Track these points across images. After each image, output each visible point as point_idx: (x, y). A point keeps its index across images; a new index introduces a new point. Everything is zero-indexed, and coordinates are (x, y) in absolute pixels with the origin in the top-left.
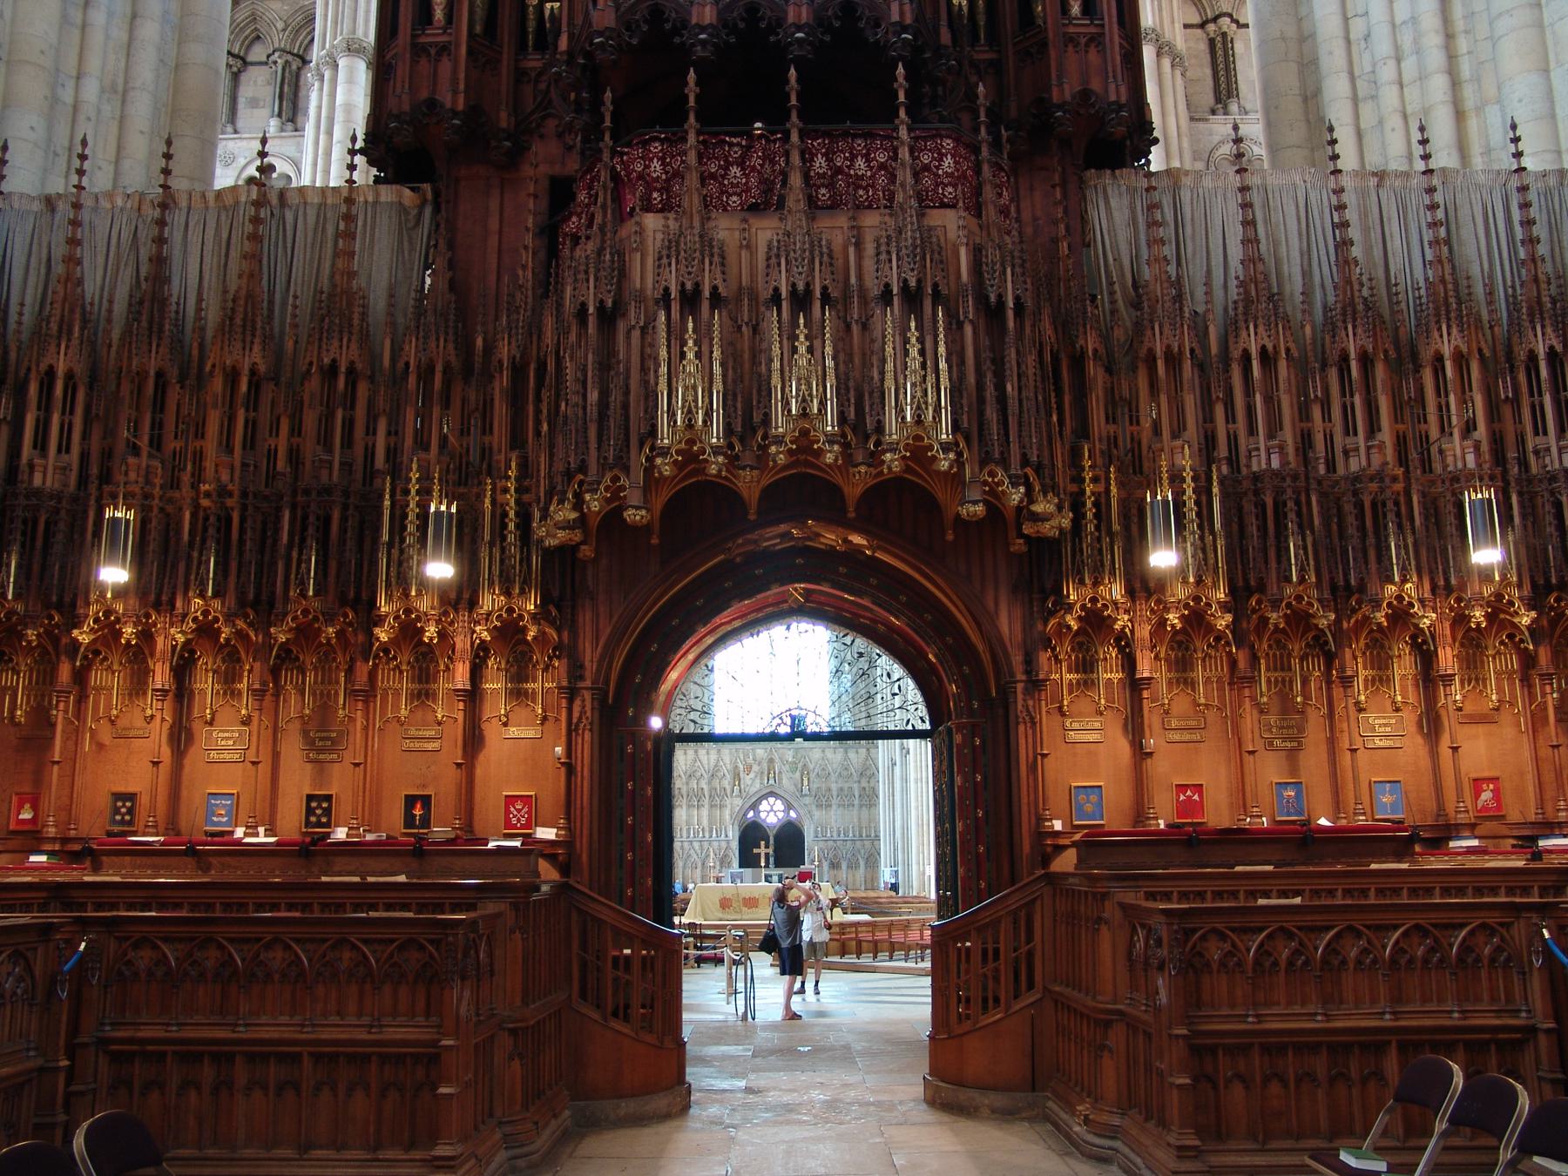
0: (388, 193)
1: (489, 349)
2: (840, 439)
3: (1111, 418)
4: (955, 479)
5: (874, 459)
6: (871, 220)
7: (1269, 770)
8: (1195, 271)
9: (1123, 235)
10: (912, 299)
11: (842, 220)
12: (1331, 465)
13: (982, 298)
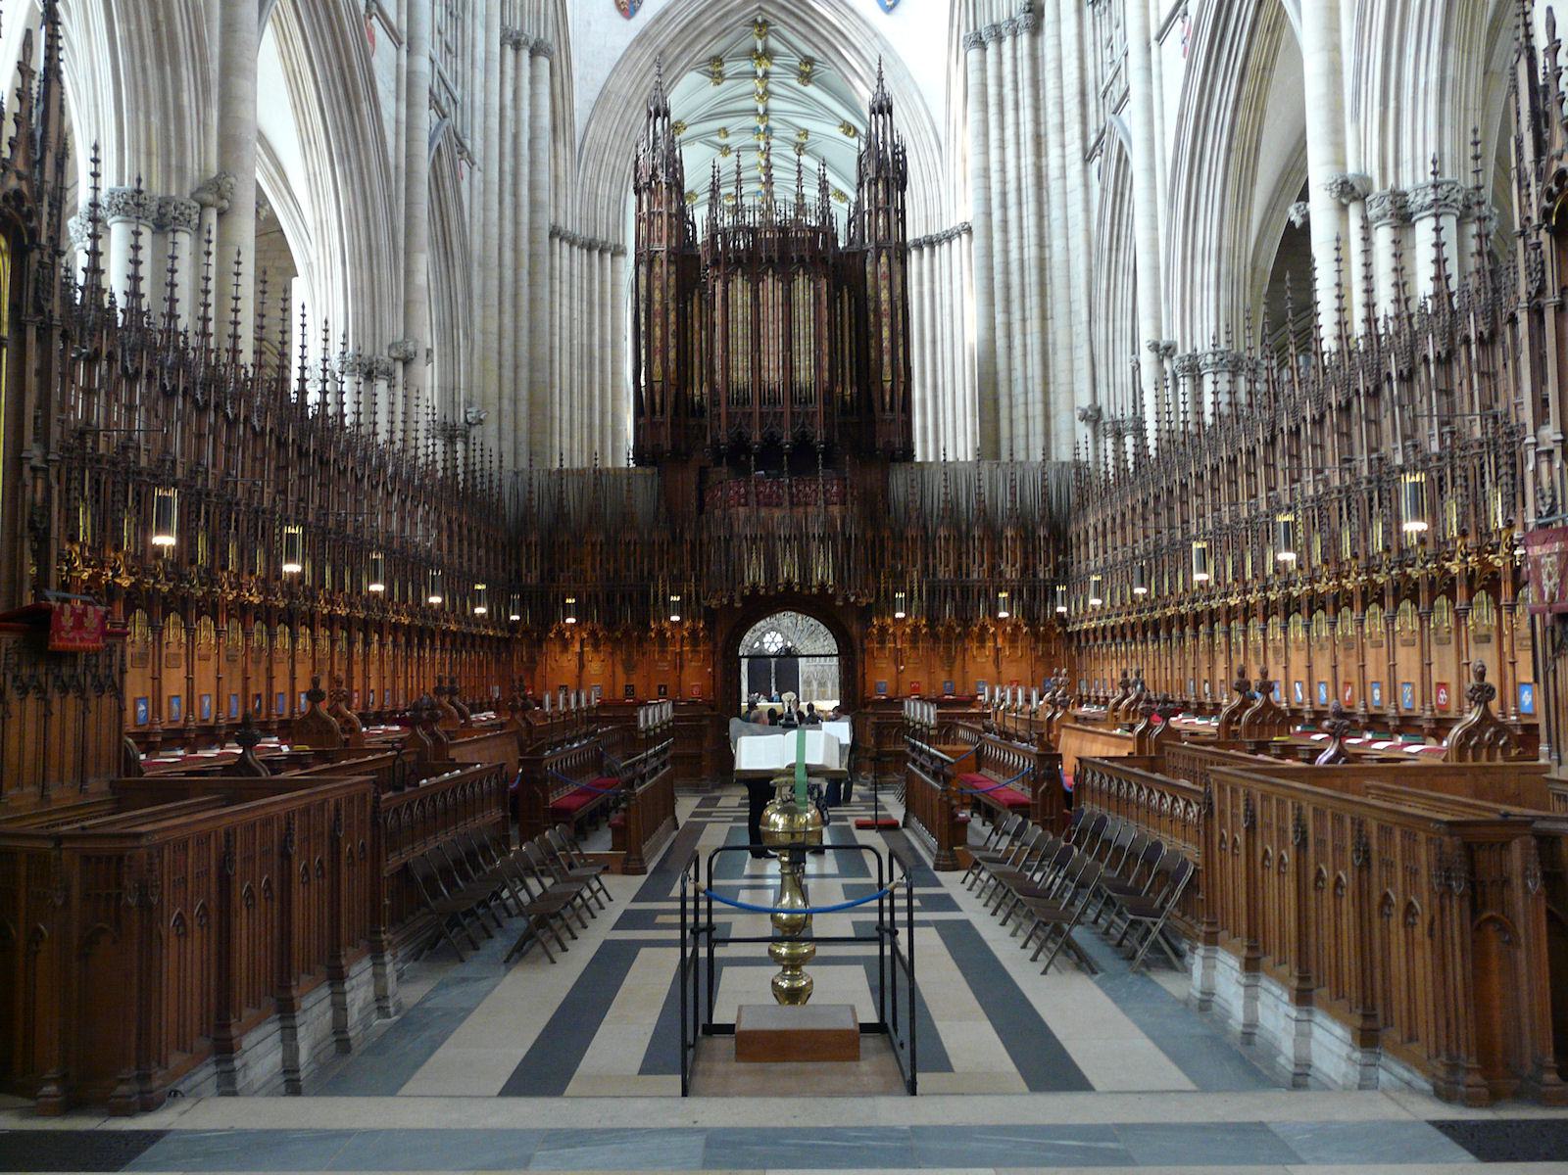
0: (640, 470)
1: (682, 532)
2: (800, 584)
3: (893, 558)
4: (833, 597)
5: (810, 588)
6: (810, 509)
7: (943, 676)
8: (928, 501)
9: (901, 490)
10: (822, 540)
11: (801, 510)
12: (968, 575)
13: (844, 534)
